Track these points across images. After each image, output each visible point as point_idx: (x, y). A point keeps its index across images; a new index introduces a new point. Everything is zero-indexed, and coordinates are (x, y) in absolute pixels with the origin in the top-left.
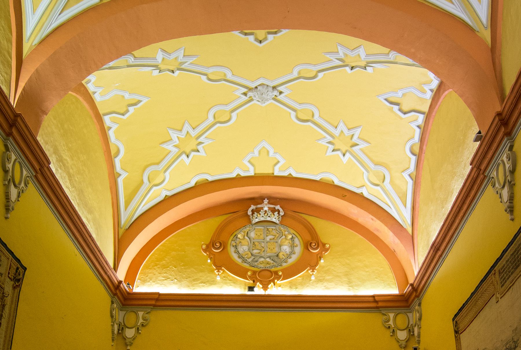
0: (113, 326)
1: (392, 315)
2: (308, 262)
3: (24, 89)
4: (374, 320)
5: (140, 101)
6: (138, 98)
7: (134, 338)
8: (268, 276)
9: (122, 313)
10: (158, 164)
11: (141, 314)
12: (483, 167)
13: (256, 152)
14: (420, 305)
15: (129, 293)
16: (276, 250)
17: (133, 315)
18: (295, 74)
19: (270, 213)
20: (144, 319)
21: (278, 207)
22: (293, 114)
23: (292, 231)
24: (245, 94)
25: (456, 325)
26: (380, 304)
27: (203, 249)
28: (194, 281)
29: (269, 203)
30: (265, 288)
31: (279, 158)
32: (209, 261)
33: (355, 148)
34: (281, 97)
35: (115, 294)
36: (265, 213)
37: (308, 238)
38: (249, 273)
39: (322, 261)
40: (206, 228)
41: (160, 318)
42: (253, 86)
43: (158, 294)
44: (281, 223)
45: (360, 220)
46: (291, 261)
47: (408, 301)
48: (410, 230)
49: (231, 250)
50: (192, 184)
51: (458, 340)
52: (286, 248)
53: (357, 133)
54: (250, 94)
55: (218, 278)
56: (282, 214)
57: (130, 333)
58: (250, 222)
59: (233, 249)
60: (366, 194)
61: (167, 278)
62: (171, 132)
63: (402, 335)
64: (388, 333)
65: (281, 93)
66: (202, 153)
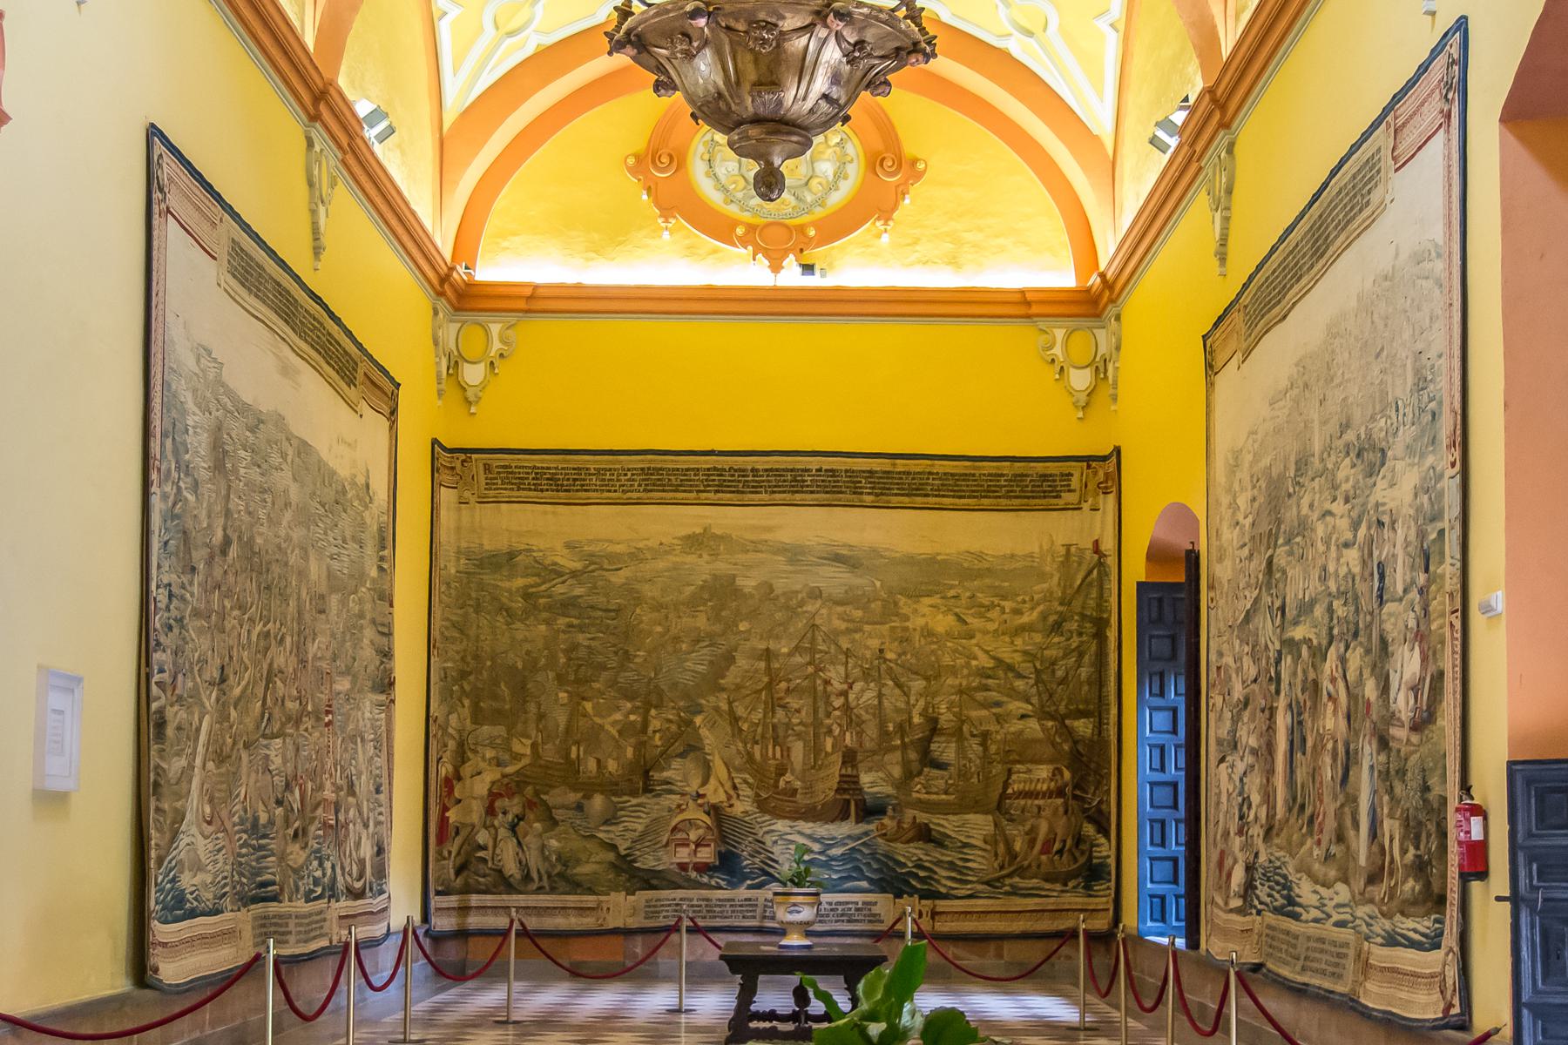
0: (438, 364)
1: (1059, 334)
7: (483, 386)
9: (454, 327)
11: (495, 329)
12: (1198, 148)
14: (1118, 318)
15: (468, 285)
20: (502, 341)
26: (1035, 309)
27: (630, 170)
30: (776, 268)
32: (645, 197)
35: (441, 294)
38: (740, 231)
39: (907, 201)
46: (837, 199)
57: (473, 374)
63: (1081, 380)
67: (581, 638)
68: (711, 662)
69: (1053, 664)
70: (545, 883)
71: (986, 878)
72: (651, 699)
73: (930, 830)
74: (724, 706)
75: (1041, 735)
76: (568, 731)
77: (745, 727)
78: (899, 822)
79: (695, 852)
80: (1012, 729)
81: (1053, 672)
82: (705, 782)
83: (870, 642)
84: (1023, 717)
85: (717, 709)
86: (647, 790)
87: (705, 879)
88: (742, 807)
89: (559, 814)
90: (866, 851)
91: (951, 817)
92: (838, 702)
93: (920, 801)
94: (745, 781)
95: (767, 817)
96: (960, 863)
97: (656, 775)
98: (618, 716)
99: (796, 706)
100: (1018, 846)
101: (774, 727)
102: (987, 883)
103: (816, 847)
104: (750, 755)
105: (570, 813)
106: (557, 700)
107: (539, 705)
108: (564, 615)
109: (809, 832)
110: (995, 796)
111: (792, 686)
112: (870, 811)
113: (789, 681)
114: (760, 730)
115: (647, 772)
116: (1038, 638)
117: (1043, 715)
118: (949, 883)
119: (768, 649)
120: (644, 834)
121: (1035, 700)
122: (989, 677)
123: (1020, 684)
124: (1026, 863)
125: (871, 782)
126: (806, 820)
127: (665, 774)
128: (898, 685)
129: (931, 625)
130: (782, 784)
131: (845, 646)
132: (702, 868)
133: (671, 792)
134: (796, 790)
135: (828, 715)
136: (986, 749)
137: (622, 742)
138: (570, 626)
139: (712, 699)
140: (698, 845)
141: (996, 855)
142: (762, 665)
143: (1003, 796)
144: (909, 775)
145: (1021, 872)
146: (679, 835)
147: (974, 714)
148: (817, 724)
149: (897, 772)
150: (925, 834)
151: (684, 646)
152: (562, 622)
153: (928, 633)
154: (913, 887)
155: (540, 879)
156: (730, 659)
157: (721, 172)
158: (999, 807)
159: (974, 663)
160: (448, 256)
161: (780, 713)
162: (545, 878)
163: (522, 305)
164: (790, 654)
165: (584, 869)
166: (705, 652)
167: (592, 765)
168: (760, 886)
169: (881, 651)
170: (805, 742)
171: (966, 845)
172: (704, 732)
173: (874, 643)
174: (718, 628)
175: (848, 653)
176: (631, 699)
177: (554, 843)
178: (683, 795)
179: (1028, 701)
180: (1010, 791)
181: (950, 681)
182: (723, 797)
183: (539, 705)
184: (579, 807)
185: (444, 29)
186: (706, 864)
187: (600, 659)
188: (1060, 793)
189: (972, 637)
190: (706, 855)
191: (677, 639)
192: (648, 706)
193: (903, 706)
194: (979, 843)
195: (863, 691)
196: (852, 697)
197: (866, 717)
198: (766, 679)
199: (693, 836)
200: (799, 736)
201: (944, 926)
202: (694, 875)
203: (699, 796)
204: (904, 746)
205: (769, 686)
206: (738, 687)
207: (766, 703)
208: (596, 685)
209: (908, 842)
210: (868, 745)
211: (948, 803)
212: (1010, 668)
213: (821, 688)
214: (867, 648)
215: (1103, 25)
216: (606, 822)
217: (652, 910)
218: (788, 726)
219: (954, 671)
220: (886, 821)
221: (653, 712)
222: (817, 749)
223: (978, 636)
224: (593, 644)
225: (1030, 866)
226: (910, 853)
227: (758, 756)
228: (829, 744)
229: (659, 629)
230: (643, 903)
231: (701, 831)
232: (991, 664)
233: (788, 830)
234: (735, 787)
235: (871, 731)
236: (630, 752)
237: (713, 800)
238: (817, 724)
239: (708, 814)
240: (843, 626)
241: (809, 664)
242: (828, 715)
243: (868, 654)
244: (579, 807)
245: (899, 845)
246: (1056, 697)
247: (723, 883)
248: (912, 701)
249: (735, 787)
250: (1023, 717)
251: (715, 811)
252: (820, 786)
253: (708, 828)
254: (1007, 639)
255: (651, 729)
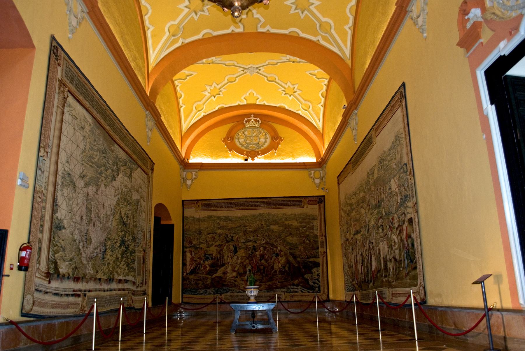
1: (313, 172)
2: (273, 147)
3: (151, 88)
4: (304, 173)
5: (192, 74)
6: (192, 73)
7: (191, 184)
8: (254, 154)
10: (200, 101)
11: (194, 173)
12: (347, 118)
13: (248, 94)
14: (325, 167)
16: (258, 140)
17: (190, 173)
18: (267, 63)
19: (254, 123)
21: (258, 119)
22: (266, 78)
23: (265, 131)
24: (243, 71)
25: (338, 181)
26: (307, 167)
28: (218, 156)
29: (254, 117)
30: (253, 159)
31: (259, 97)
33: (296, 94)
34: (260, 72)
35: (181, 165)
36: (253, 123)
37: (273, 134)
40: (224, 130)
41: (203, 174)
42: (247, 67)
43: (202, 164)
44: (260, 127)
45: (298, 125)
47: (321, 164)
48: (321, 132)
49: (236, 141)
50: (217, 109)
51: (339, 187)
52: (262, 140)
53: (296, 86)
54: (245, 71)
55: (230, 155)
56: (260, 122)
57: (189, 182)
58: (245, 127)
59: (237, 140)
60: (301, 113)
61: (205, 155)
62: (206, 86)
63: (317, 181)
64: (311, 180)
65: (260, 70)
66: (222, 95)
157: (241, 141)
160: (183, 156)
163: (199, 167)
185: (182, 110)
215: (320, 106)
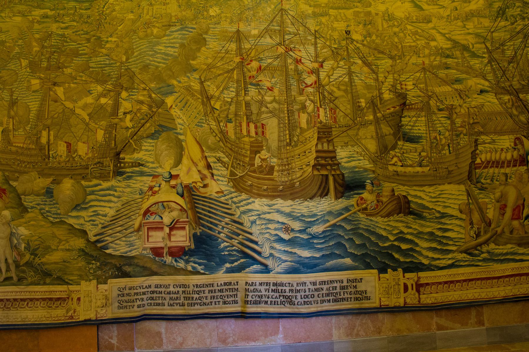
67: (54, 27)
68: (182, 46)
69: (503, 45)
70: (13, 274)
71: (463, 248)
72: (123, 82)
73: (409, 202)
74: (196, 86)
75: (499, 108)
76: (40, 116)
77: (217, 106)
78: (378, 195)
79: (169, 235)
80: (474, 103)
81: (503, 51)
82: (178, 162)
83: (336, 25)
84: (482, 92)
85: (188, 89)
86: (118, 173)
87: (181, 264)
88: (218, 186)
89: (28, 201)
90: (348, 227)
91: (426, 189)
92: (310, 80)
93: (397, 173)
94: (219, 160)
95: (244, 196)
96: (439, 233)
97: (127, 158)
98: (89, 100)
99: (269, 85)
100: (491, 214)
101: (248, 105)
102: (466, 252)
103: (297, 225)
104: (224, 134)
105: (38, 199)
106: (28, 88)
107: (12, 93)
108: (39, 7)
109: (288, 210)
110: (465, 167)
111: (264, 65)
112: (349, 186)
113: (260, 60)
114: (233, 108)
115: (118, 154)
116: (486, 22)
117: (499, 89)
118: (431, 254)
119: (238, 31)
120: (115, 219)
121: (490, 77)
122: (448, 56)
123: (475, 63)
124: (499, 230)
125: (349, 157)
126: (284, 197)
127: (136, 156)
128: (367, 64)
129: (390, 12)
130: (257, 162)
131: (313, 29)
132: (178, 253)
133: (142, 174)
134: (272, 168)
135: (301, 92)
136: (453, 123)
137: (92, 125)
138: (46, 16)
139: (183, 79)
140: (171, 229)
141: (471, 223)
142: (233, 46)
143: (473, 167)
144: (384, 149)
145: (495, 238)
146: (152, 219)
147: (438, 90)
148: (290, 102)
149: (372, 146)
150: (404, 207)
151: (155, 31)
152: (37, 13)
153: (389, 17)
154: (397, 260)
155: (8, 270)
156: (200, 41)
158: (470, 177)
159: (433, 44)
161: (253, 91)
162: (13, 267)
164: (261, 36)
165: (54, 257)
166: (176, 36)
167: (62, 149)
168: (240, 269)
169: (348, 32)
170: (279, 118)
171: (444, 215)
172: (175, 112)
173: (341, 26)
174: (189, 14)
175: (316, 35)
176: (103, 82)
177: (23, 231)
178: (155, 176)
179: (485, 78)
180: (478, 161)
181: (414, 60)
182: (196, 177)
183: (12, 93)
184: (49, 193)
186: (182, 248)
187: (73, 45)
188: (523, 161)
189: (431, 22)
190: (182, 238)
191: (148, 24)
192: (119, 87)
193: (372, 82)
194: (456, 213)
195: (333, 69)
196: (323, 75)
197: (338, 93)
198: (238, 60)
199: (167, 219)
200: (273, 113)
201: (429, 298)
202: (169, 260)
203: (172, 177)
204: (377, 121)
205: (242, 65)
206: (210, 67)
207: (238, 81)
208: (68, 71)
209: (388, 215)
210: (342, 120)
211: (424, 175)
212: (465, 48)
213: (292, 67)
214: (334, 29)
216: (76, 207)
217: (125, 298)
218: (261, 103)
219: (417, 52)
220: (366, 195)
221: (124, 94)
222: (291, 126)
223: (434, 20)
224: (66, 32)
225: (503, 232)
226: (388, 226)
227: (231, 135)
228: (303, 119)
229: (131, 16)
230: (116, 293)
231: (175, 214)
232: (449, 45)
233: (266, 209)
234: (209, 167)
235: (344, 106)
236: (100, 135)
237: (186, 180)
238: (290, 102)
239: (182, 196)
240: (310, 10)
241: (280, 44)
242: (301, 92)
243: (336, 35)
244: (49, 193)
245: (379, 219)
246: (509, 74)
247: (199, 268)
248: (381, 77)
249: (209, 167)
250: (482, 92)
251: (188, 192)
252: (297, 164)
253: (182, 210)
254: (460, 24)
255: (121, 110)
